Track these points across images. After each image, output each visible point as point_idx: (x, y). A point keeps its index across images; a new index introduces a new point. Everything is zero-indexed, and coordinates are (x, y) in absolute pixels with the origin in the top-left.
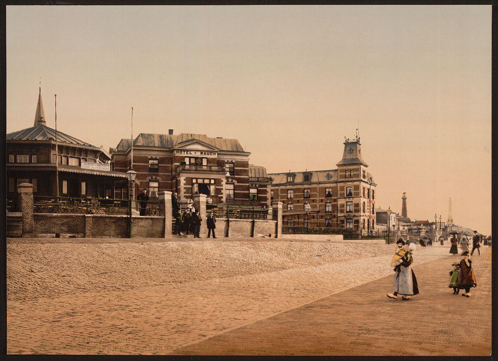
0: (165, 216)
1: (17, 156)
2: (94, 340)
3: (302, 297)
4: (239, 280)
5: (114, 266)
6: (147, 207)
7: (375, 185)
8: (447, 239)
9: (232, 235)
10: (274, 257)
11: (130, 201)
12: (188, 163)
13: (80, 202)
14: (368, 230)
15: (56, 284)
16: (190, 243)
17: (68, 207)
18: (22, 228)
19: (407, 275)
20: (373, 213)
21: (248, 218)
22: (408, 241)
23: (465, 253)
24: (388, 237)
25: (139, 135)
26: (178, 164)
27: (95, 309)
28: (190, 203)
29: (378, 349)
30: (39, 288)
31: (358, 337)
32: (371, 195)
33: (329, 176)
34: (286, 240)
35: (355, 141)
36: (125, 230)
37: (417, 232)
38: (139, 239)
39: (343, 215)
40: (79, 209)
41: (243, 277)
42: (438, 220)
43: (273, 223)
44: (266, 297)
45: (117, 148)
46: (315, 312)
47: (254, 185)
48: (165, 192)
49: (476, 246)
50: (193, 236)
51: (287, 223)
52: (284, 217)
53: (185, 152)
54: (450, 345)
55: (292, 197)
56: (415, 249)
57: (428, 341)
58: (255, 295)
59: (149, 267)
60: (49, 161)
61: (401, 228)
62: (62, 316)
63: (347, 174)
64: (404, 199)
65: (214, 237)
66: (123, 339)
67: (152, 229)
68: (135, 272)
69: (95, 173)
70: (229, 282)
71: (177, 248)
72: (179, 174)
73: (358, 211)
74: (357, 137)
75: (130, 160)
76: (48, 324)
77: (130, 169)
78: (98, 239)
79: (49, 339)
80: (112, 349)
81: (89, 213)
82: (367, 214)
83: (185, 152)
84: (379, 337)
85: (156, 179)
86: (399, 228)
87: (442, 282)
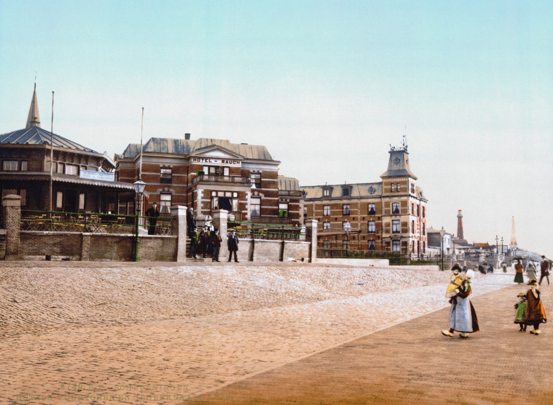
0: (178, 235)
1: (4, 162)
2: (87, 387)
3: (341, 334)
4: (265, 313)
5: (116, 295)
6: (157, 225)
7: (426, 201)
8: (510, 266)
9: (258, 259)
10: (307, 285)
11: (137, 217)
12: (206, 172)
13: (77, 218)
14: (418, 253)
15: (44, 317)
16: (207, 268)
17: (62, 224)
18: (5, 248)
19: (464, 308)
20: (424, 234)
21: (277, 239)
22: (465, 267)
23: (533, 282)
24: (441, 262)
25: (150, 140)
26: (195, 174)
27: (89, 348)
28: (208, 221)
29: (432, 399)
30: (22, 322)
31: (408, 384)
32: (421, 212)
33: (372, 190)
34: (321, 265)
35: (402, 149)
36: (129, 252)
37: (475, 257)
38: (147, 262)
39: (388, 235)
40: (76, 226)
41: (270, 310)
42: (500, 243)
43: (306, 244)
44: (298, 334)
45: (124, 154)
46: (356, 352)
47: (284, 200)
48: (179, 207)
49: (544, 274)
50: (211, 259)
51: (323, 245)
52: (319, 237)
53: (204, 160)
54: (518, 394)
55: (329, 213)
56: (473, 277)
57: (491, 388)
58: (284, 332)
59: (157, 296)
60: (41, 169)
61: (457, 252)
62: (48, 357)
63: (393, 188)
64: (460, 218)
65: (236, 260)
66: (123, 386)
67: (163, 251)
68: (141, 303)
69: (96, 184)
70: (253, 316)
71: (192, 273)
72: (196, 186)
73: (405, 231)
74: (404, 145)
75: (139, 169)
76: (31, 367)
77: (138, 180)
78: (97, 263)
79: (32, 386)
80: (109, 398)
81: (87, 231)
82: (417, 235)
83: (204, 160)
84: (432, 384)
85: (168, 191)
86: (454, 252)
87: (506, 317)
